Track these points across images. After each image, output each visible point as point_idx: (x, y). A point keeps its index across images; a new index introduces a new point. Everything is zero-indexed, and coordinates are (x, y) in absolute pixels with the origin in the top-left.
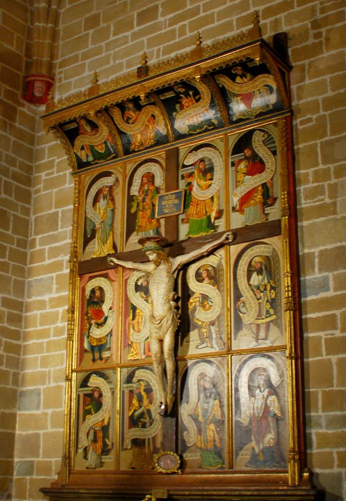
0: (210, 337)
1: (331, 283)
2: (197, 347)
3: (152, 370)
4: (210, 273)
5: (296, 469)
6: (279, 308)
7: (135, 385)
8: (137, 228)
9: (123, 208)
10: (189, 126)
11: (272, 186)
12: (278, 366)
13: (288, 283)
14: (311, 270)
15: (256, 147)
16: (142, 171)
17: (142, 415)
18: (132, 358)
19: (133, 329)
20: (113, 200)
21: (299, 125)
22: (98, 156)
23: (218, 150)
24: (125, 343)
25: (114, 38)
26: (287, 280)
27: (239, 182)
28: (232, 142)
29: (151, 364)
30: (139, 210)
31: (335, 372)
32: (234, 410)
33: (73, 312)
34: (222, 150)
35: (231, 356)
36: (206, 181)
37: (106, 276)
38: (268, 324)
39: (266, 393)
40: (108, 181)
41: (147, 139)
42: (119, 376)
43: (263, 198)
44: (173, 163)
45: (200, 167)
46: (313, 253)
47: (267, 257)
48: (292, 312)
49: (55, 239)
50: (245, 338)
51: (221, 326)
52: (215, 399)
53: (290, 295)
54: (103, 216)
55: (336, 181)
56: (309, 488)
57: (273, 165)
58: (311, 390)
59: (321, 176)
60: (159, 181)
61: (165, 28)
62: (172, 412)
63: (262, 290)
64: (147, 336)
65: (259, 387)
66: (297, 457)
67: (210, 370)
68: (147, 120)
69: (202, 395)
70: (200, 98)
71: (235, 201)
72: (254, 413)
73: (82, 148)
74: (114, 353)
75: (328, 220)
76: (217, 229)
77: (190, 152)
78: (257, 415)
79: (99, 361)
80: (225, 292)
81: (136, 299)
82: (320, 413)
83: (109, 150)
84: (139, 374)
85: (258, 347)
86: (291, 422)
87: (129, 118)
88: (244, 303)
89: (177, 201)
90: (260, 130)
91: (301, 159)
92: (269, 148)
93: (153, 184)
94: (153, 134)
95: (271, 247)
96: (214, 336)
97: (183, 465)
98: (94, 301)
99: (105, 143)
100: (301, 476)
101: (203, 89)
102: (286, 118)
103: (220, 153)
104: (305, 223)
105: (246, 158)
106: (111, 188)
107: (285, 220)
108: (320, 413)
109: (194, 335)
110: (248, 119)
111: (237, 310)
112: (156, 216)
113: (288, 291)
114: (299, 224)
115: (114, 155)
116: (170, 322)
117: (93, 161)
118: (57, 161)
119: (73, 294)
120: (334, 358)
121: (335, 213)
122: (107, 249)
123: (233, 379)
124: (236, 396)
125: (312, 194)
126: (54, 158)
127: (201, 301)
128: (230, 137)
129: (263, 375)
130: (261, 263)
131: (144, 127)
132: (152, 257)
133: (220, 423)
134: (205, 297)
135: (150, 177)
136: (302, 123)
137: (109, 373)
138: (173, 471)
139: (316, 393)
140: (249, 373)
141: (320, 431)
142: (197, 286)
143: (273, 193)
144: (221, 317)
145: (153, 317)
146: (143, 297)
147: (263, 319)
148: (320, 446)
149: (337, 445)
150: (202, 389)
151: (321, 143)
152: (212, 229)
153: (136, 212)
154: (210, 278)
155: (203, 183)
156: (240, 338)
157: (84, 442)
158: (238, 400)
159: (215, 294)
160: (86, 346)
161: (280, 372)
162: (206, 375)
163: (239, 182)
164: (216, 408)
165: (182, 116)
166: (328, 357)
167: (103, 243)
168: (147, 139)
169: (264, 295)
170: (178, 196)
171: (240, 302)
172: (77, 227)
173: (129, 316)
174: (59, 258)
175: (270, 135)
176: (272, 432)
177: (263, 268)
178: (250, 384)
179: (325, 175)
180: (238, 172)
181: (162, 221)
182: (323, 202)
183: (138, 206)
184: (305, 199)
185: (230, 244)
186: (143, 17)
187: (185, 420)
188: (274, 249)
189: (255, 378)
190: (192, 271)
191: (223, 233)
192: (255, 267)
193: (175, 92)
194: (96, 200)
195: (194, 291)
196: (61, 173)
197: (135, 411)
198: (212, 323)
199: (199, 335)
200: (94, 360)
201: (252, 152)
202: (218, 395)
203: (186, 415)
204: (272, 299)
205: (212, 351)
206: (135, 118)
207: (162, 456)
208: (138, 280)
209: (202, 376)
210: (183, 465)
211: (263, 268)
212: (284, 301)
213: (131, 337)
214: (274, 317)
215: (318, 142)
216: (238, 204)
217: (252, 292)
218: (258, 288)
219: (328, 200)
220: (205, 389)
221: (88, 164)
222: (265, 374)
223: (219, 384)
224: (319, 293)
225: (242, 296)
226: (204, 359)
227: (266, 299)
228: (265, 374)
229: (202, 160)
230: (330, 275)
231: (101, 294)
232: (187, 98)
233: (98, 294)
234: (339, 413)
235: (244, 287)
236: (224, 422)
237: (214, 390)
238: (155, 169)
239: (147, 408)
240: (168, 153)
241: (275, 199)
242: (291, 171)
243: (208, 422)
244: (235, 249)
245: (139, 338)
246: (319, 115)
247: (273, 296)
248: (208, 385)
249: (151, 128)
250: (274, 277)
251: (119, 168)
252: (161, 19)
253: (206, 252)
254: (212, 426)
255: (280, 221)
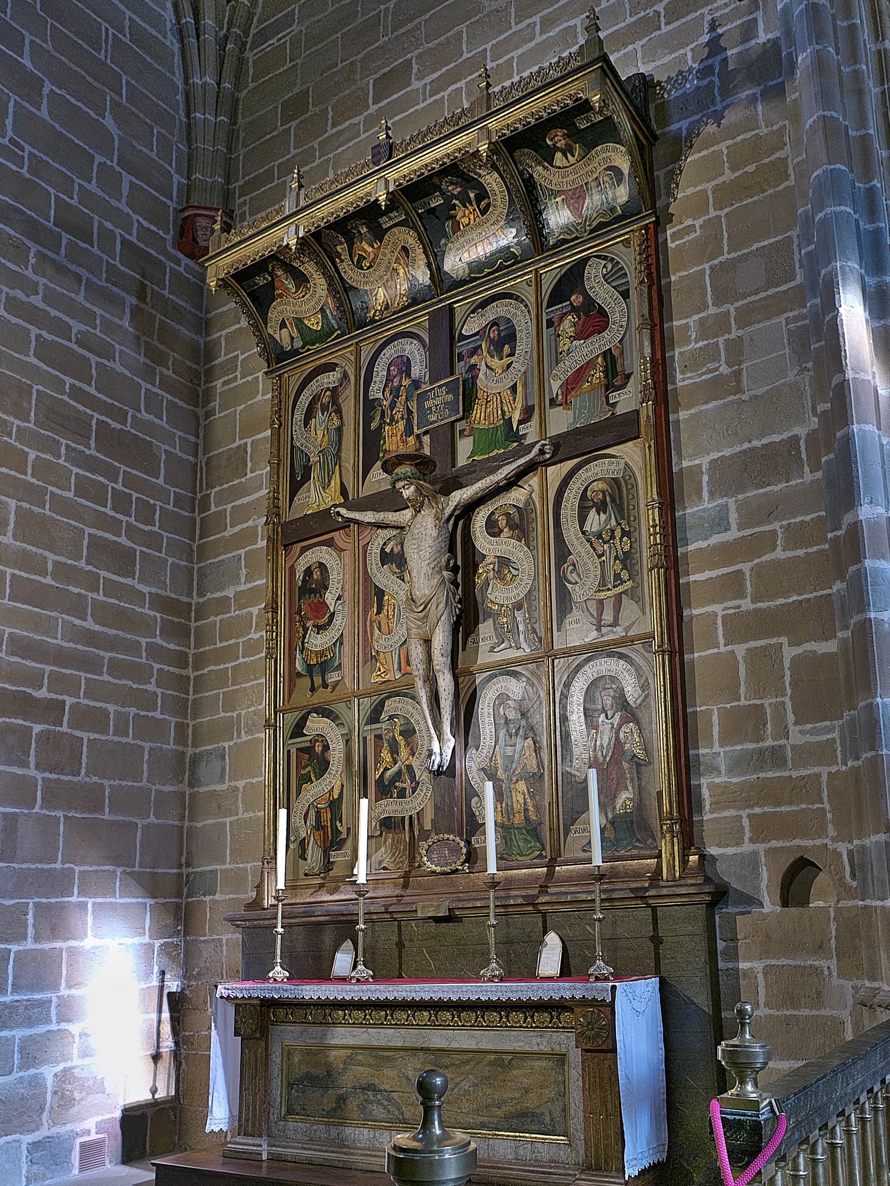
0: (514, 630)
1: (733, 517)
2: (492, 650)
3: (413, 698)
4: (513, 519)
5: (676, 848)
6: (637, 567)
7: (384, 726)
8: (381, 455)
9: (357, 423)
10: (469, 264)
11: (622, 353)
12: (638, 670)
13: (654, 520)
14: (694, 497)
15: (591, 288)
16: (388, 355)
17: (398, 775)
18: (379, 679)
19: (380, 630)
20: (339, 411)
21: (669, 241)
22: (311, 338)
23: (522, 301)
24: (365, 654)
25: (335, 130)
26: (653, 514)
27: (561, 353)
28: (548, 284)
29: (412, 686)
30: (385, 422)
31: (742, 673)
32: (559, 754)
33: (275, 611)
34: (531, 300)
35: (553, 660)
36: (502, 359)
37: (330, 543)
38: (619, 598)
39: (616, 720)
40: (330, 379)
41: (396, 296)
43: (606, 377)
45: (492, 335)
46: (699, 466)
47: (615, 480)
48: (662, 570)
49: (243, 491)
50: (576, 626)
51: (534, 608)
52: (526, 738)
53: (658, 541)
54: (322, 441)
55: (740, 332)
56: (700, 880)
58: (698, 709)
60: (418, 370)
61: (424, 100)
63: (607, 538)
64: (403, 640)
65: (604, 711)
66: (676, 828)
67: (515, 688)
68: (394, 258)
69: (502, 733)
70: (488, 205)
71: (556, 386)
72: (596, 757)
73: (283, 325)
75: (725, 406)
76: (523, 441)
77: (473, 312)
78: (601, 759)
79: (321, 689)
80: (540, 549)
81: (384, 577)
82: (716, 748)
83: (329, 323)
84: (392, 705)
85: (602, 639)
86: (664, 765)
87: (361, 258)
88: (574, 565)
89: (450, 397)
90: (599, 257)
92: (613, 287)
93: (408, 375)
94: (405, 286)
95: (623, 461)
96: (521, 628)
99: (322, 310)
100: (684, 861)
101: (492, 181)
102: (646, 227)
103: (526, 306)
105: (574, 309)
106: (334, 390)
107: (647, 410)
108: (716, 748)
109: (486, 629)
110: (576, 238)
111: (561, 580)
112: (415, 430)
113: (655, 534)
114: (672, 417)
115: (339, 332)
116: (442, 605)
117: (303, 348)
118: (241, 358)
119: (275, 579)
120: (740, 650)
121: (739, 390)
122: (329, 498)
123: (557, 700)
124: (563, 729)
125: (695, 362)
126: (236, 353)
127: (496, 569)
128: (543, 276)
129: (611, 688)
130: (603, 492)
131: (389, 274)
132: (408, 492)
133: (535, 779)
134: (504, 562)
135: (405, 365)
136: (675, 237)
137: (340, 708)
138: (453, 867)
139: (709, 713)
140: (585, 687)
141: (717, 780)
142: (490, 543)
143: (623, 365)
144: (534, 593)
145: (412, 599)
146: (396, 573)
147: (609, 590)
148: (717, 806)
149: (748, 803)
150: (503, 722)
151: (712, 268)
152: (514, 442)
153: (380, 428)
154: (512, 526)
155: (496, 363)
156: (568, 627)
158: (566, 737)
159: (521, 555)
160: (299, 666)
161: (642, 681)
162: (508, 698)
163: (561, 353)
164: (527, 754)
165: (457, 245)
166: (730, 648)
167: (323, 488)
168: (396, 296)
169: (610, 548)
170: (451, 388)
171: (566, 565)
172: (278, 464)
173: (372, 607)
174: (250, 523)
175: (618, 262)
176: (630, 788)
177: (608, 499)
178: (588, 706)
179: (721, 324)
180: (559, 336)
181: (426, 439)
182: (717, 373)
183: (383, 416)
184: (682, 373)
185: (546, 464)
186: (384, 87)
187: (473, 778)
188: (626, 464)
189: (597, 695)
190: (480, 519)
191: (533, 445)
192: (592, 500)
193: (443, 194)
194: (309, 415)
195: (484, 552)
196: (250, 378)
197: (386, 769)
198: (518, 606)
199: (495, 629)
200: (313, 689)
201: (584, 298)
202: (531, 731)
203: (475, 769)
204: (624, 553)
205: (519, 653)
206: (372, 256)
207: (434, 843)
208: (385, 544)
209: (502, 699)
211: (608, 499)
212: (646, 554)
213: (375, 644)
214: (629, 584)
215: (707, 266)
216: (560, 393)
217: (588, 545)
218: (599, 536)
219: (724, 370)
220: (507, 722)
221: (295, 352)
222: (614, 686)
223: (532, 711)
224: (711, 536)
225: (571, 554)
226: (506, 669)
227: (614, 554)
228: (614, 686)
229: (494, 323)
230: (731, 501)
231: (321, 575)
232: (465, 206)
233: (316, 575)
234: (752, 746)
235: (573, 538)
236: (542, 774)
237: (523, 723)
238: (412, 349)
239: (407, 763)
240: (434, 317)
241: (628, 376)
242: (657, 321)
243: (514, 779)
244: (555, 473)
245: (390, 643)
246: (707, 217)
247: (627, 548)
248: (512, 715)
249: (401, 274)
250: (628, 513)
251: (348, 355)
252: (416, 85)
253: (505, 478)
254: (522, 786)
255: (637, 412)
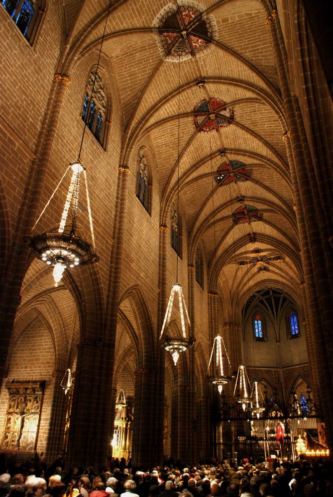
40: (15, 398)
42: (11, 433)
44: (25, 398)
49: (4, 406)
57: (39, 402)
59: (46, 406)
60: (23, 400)
62: (19, 440)
71: (33, 407)
74: (11, 429)
81: (16, 420)
91: (44, 403)
97: (19, 449)
98: (9, 420)
104: (42, 413)
109: (24, 428)
122: (13, 411)
135: (22, 399)
157: (4, 444)
210: (19, 449)
226: (25, 432)
238: (23, 398)
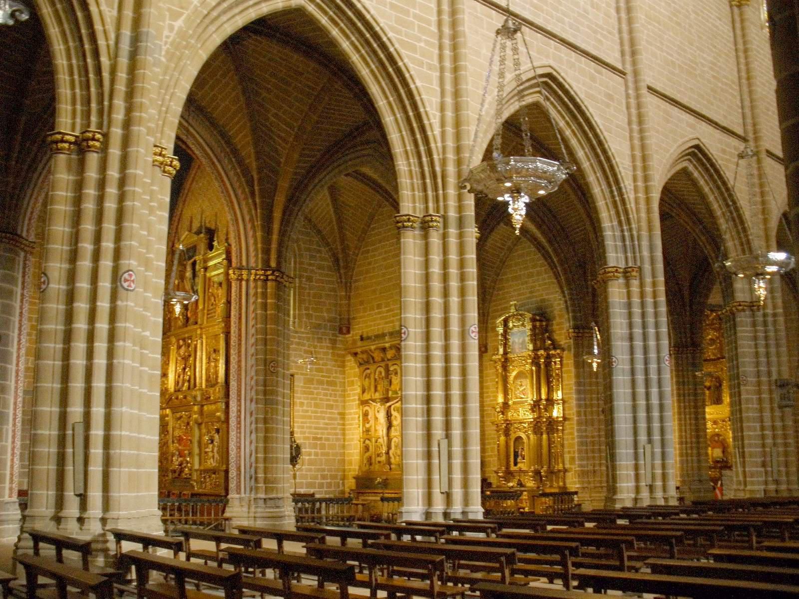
40: (368, 371)
42: (373, 440)
49: (354, 390)
60: (383, 374)
62: (387, 453)
74: (372, 433)
97: (390, 469)
98: (366, 415)
135: (381, 373)
190: (393, 407)
210: (390, 469)
